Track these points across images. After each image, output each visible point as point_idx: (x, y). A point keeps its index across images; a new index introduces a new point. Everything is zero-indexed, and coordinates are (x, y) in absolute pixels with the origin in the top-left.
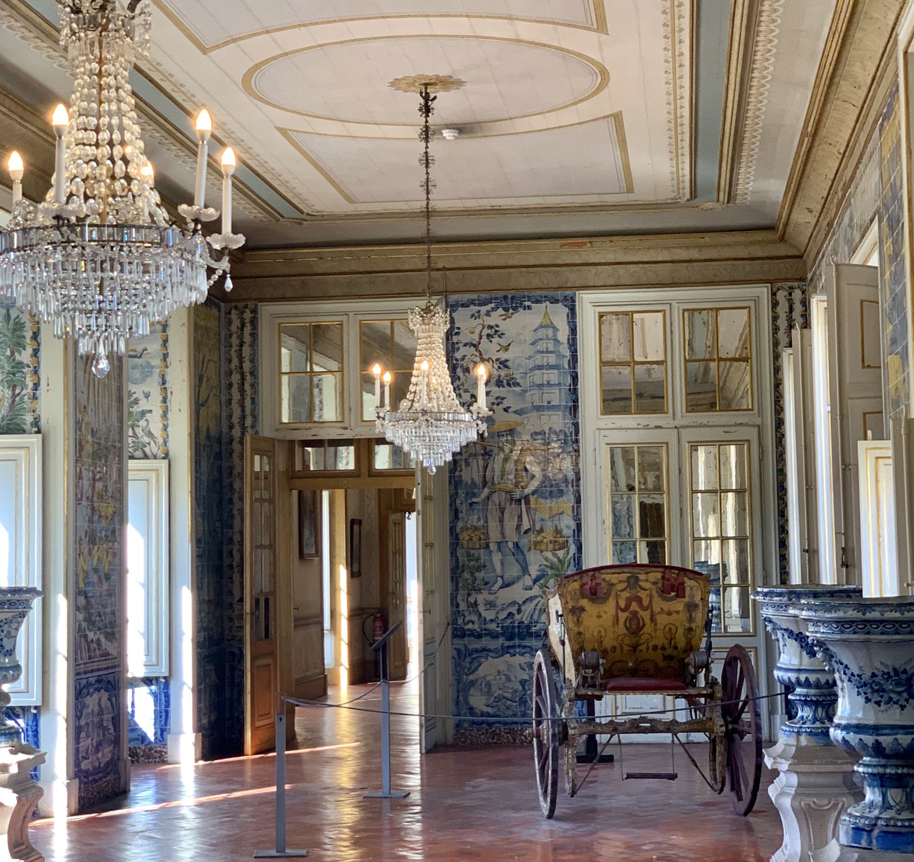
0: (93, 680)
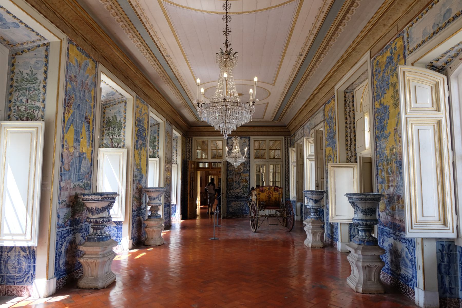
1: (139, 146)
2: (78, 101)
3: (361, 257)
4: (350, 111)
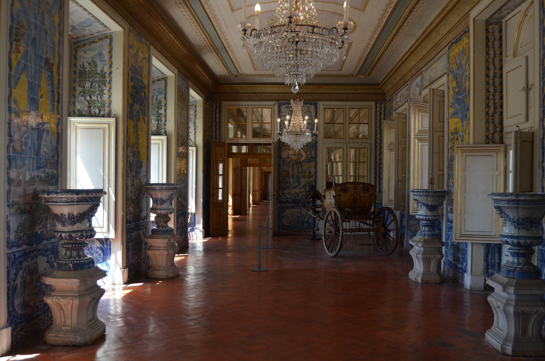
0: (180, 213)
1: (135, 113)
2: (33, 31)
3: (513, 297)
4: (495, 56)
